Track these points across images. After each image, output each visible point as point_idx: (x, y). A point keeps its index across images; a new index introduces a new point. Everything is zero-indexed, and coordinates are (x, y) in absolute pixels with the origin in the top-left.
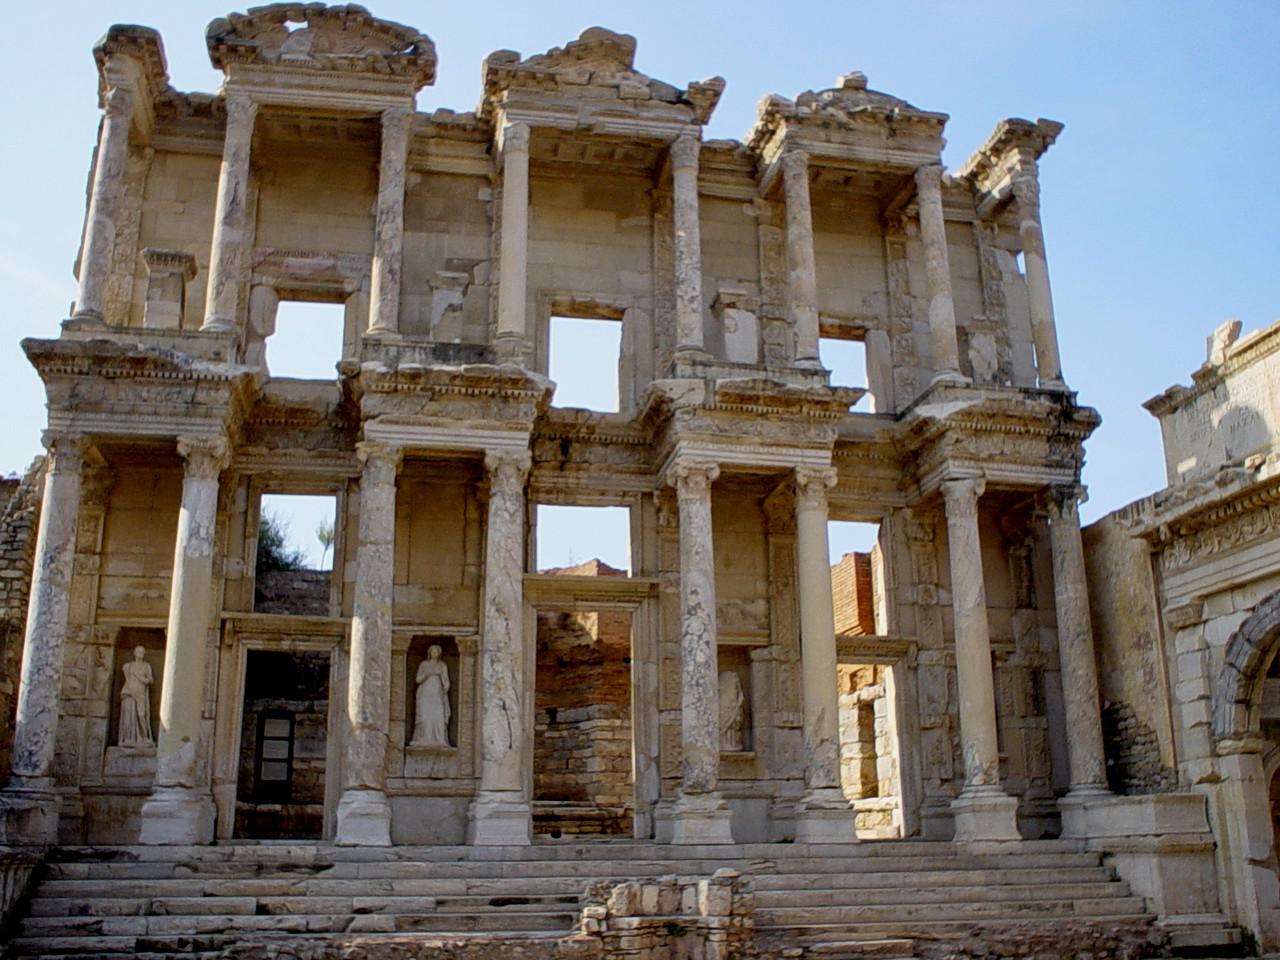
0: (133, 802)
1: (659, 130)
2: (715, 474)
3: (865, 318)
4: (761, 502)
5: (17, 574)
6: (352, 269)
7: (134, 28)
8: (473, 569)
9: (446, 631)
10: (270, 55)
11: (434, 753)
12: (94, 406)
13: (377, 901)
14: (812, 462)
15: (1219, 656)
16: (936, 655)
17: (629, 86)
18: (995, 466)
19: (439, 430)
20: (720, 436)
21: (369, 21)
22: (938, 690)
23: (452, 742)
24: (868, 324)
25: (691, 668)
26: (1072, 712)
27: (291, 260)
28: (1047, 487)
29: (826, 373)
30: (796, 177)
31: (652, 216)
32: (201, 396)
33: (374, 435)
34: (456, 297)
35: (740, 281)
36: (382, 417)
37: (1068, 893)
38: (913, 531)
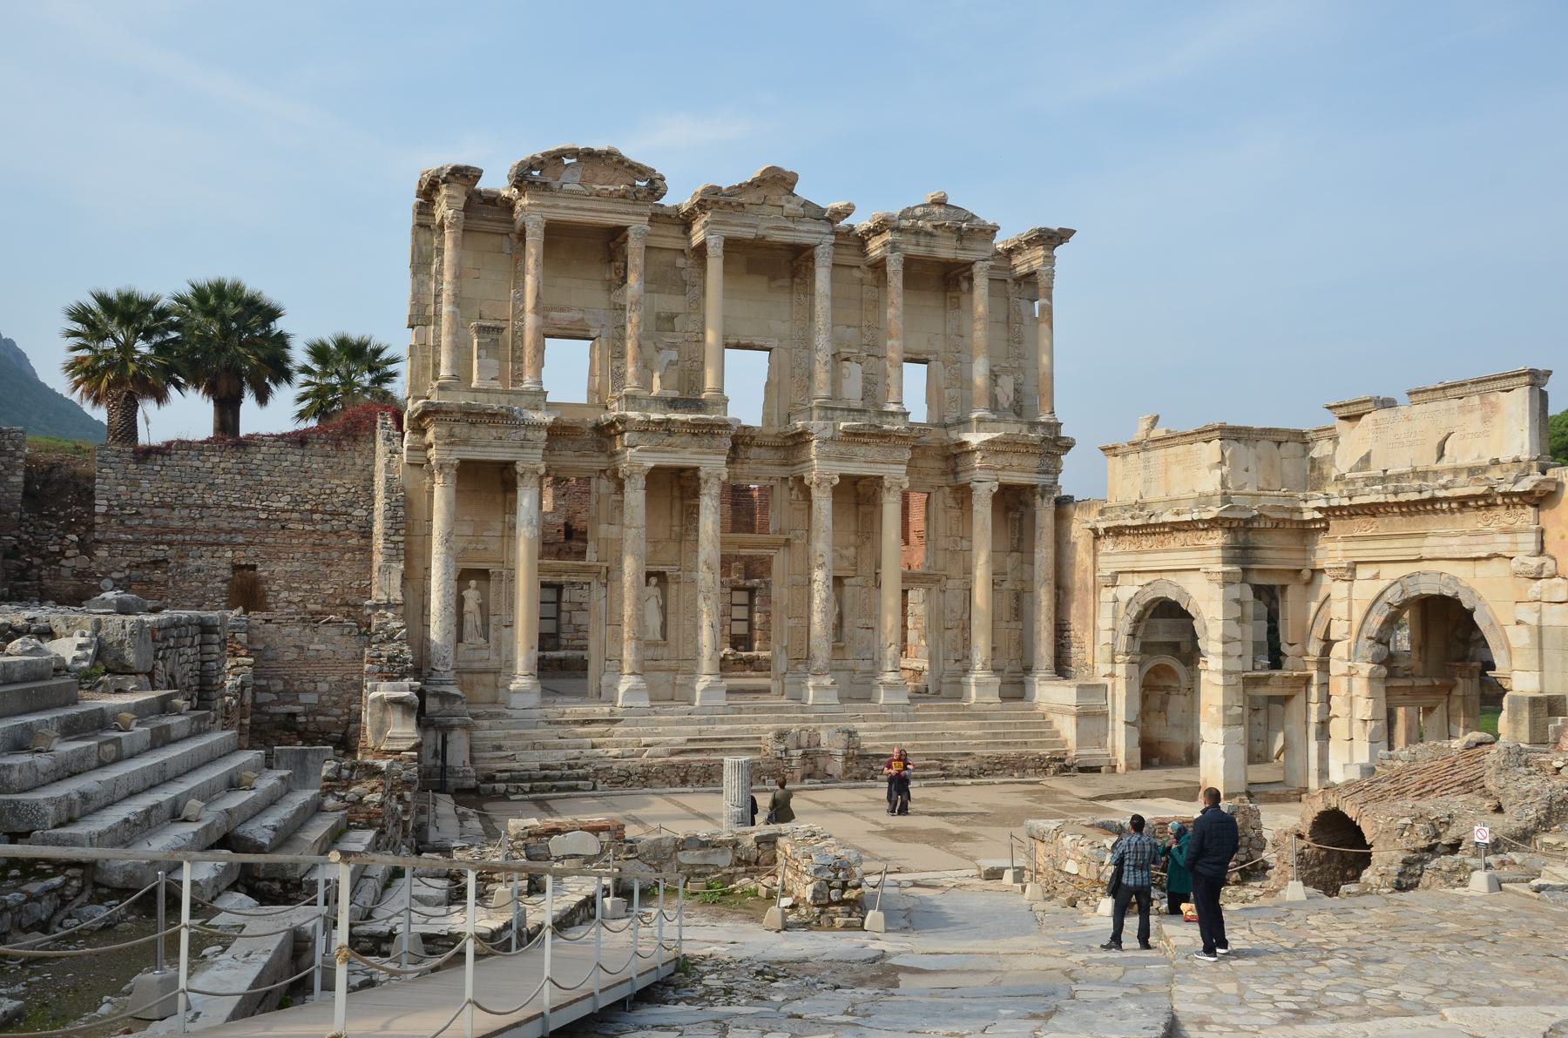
0: (476, 678)
2: (837, 481)
3: (929, 353)
4: (855, 483)
7: (467, 168)
8: (676, 529)
9: (660, 568)
10: (556, 185)
11: (656, 644)
12: (465, 442)
14: (894, 471)
15: (1122, 606)
16: (958, 582)
17: (790, 207)
20: (841, 458)
21: (622, 161)
22: (957, 604)
23: (664, 637)
27: (554, 314)
29: (906, 414)
30: (895, 272)
31: (793, 276)
32: (530, 435)
34: (674, 355)
38: (950, 502)
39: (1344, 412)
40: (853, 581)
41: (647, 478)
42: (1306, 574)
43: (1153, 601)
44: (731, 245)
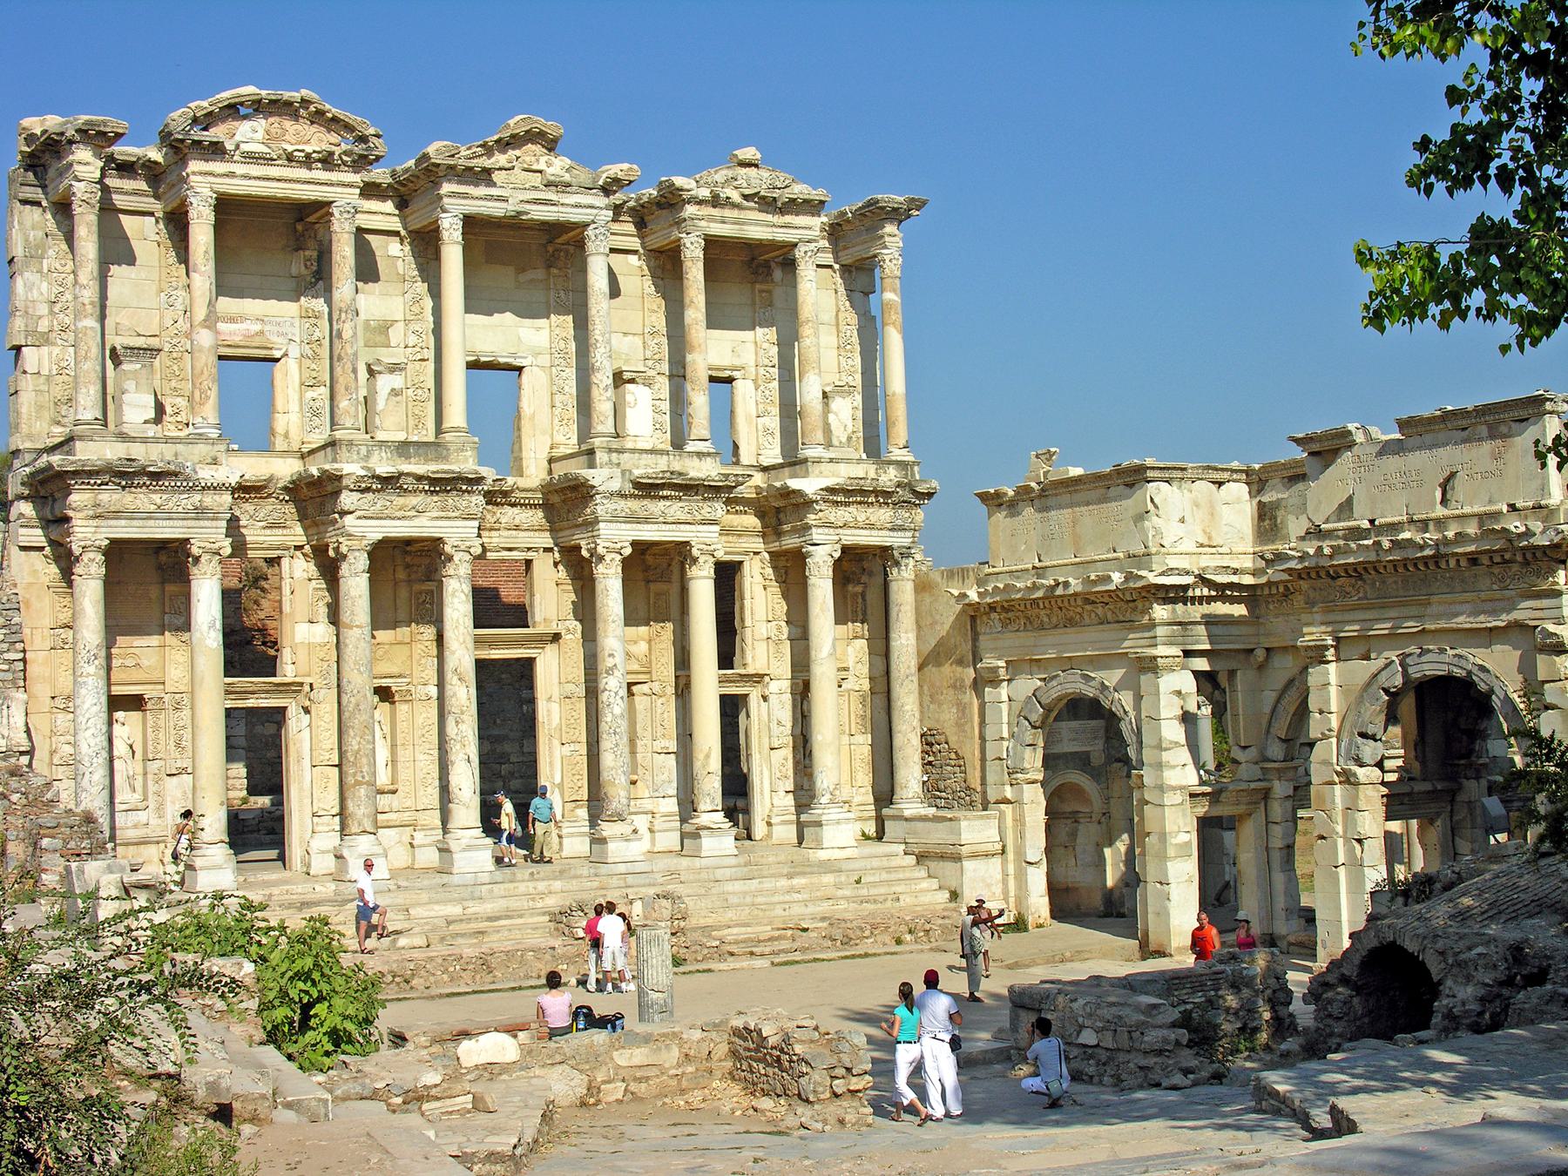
1: (575, 216)
2: (628, 551)
5: (21, 656)
6: (280, 334)
7: (105, 124)
9: (384, 682)
10: (229, 146)
12: (117, 514)
13: (406, 925)
18: (849, 532)
19: (406, 523)
21: (320, 113)
24: (736, 374)
25: (609, 719)
26: (898, 740)
28: (891, 548)
33: (352, 530)
35: (625, 334)
36: (358, 513)
37: (894, 889)
39: (1316, 447)
40: (645, 688)
41: (371, 555)
42: (1260, 654)
43: (1059, 699)
44: (471, 224)
